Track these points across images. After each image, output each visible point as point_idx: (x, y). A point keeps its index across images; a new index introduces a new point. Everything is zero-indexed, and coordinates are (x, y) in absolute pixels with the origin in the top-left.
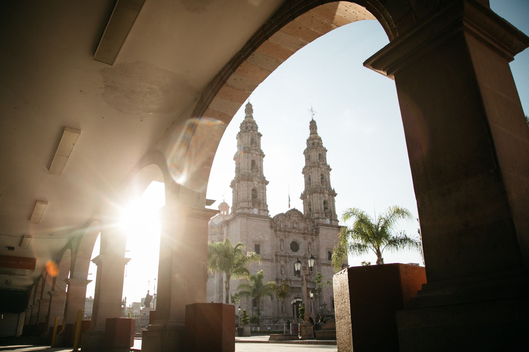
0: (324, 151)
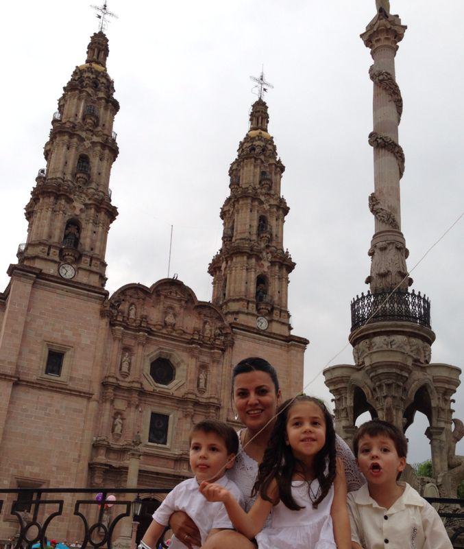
0: (276, 167)
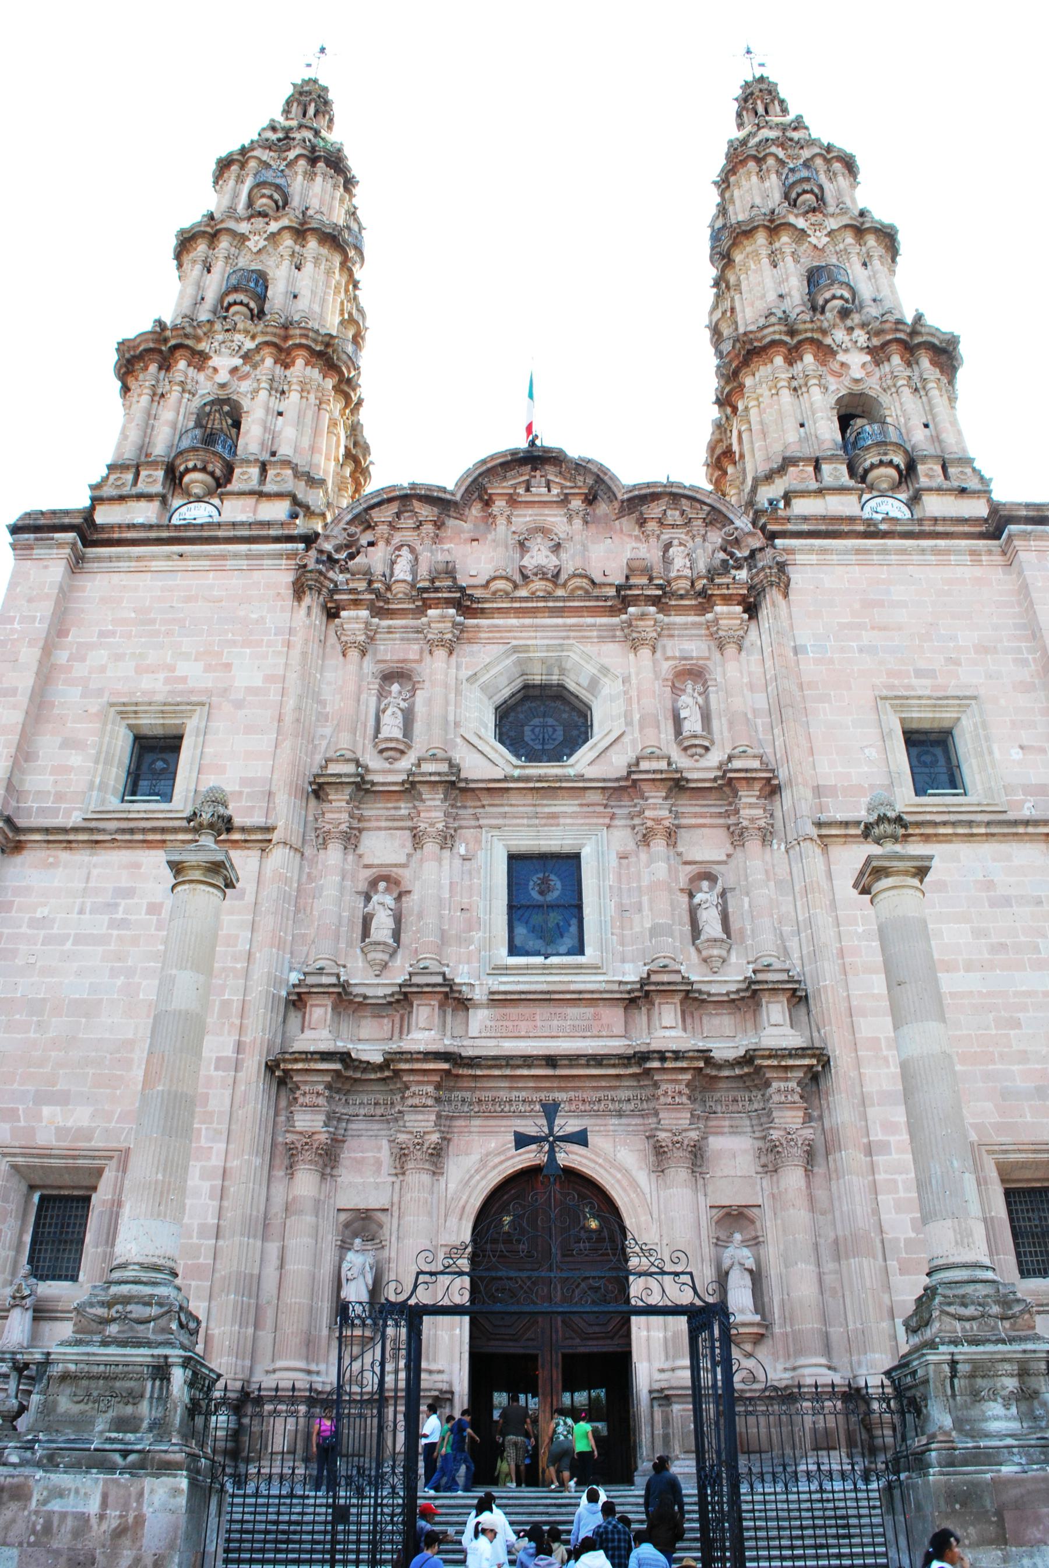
0: (828, 161)
